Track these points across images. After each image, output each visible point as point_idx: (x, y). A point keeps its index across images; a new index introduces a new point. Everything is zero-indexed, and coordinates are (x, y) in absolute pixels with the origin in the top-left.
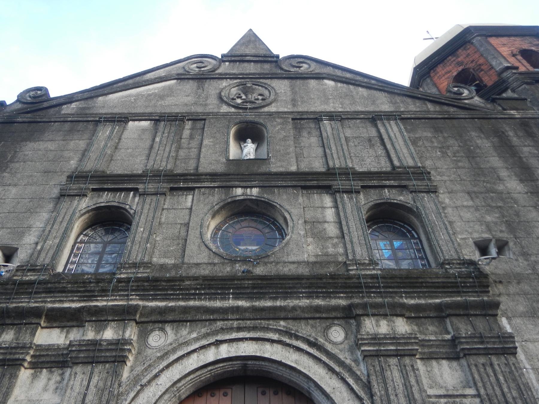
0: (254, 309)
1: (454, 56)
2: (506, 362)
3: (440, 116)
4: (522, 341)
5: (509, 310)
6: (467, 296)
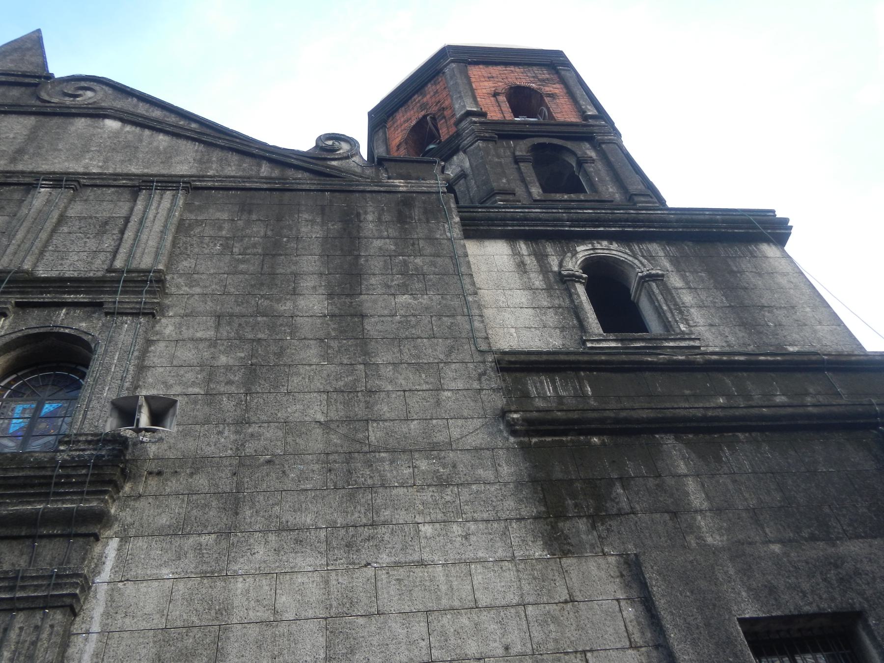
1: (421, 94)
2: (40, 624)
3: (265, 186)
4: (121, 581)
5: (137, 524)
6: (59, 501)
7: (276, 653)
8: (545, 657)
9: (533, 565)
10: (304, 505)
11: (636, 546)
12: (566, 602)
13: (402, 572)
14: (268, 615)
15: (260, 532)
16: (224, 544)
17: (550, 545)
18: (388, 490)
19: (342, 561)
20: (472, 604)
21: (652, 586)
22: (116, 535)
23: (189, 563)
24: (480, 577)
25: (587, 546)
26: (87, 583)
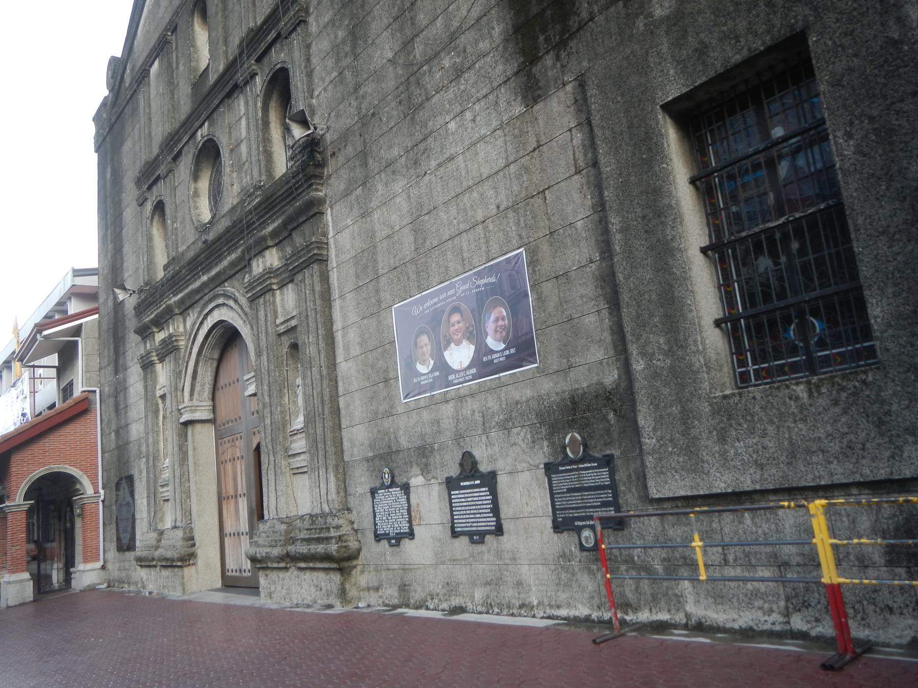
0: (212, 280)
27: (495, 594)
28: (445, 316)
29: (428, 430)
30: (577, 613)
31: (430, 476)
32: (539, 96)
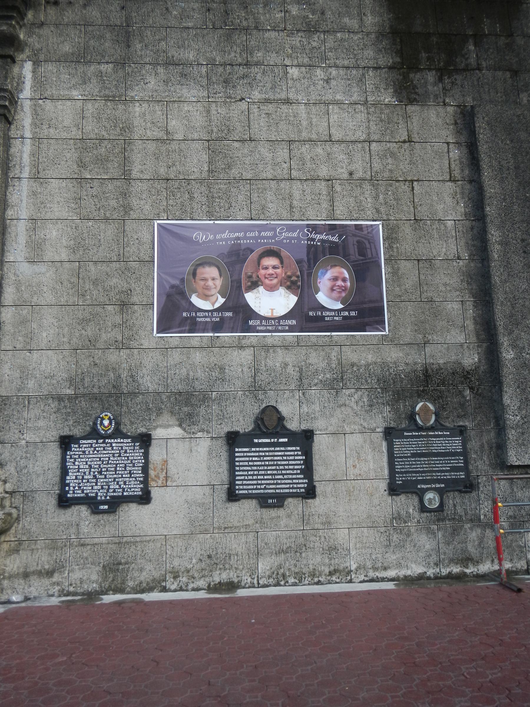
5: (44, 50)
7: (170, 164)
8: (380, 182)
9: (382, 109)
10: (186, 42)
11: (474, 99)
12: (404, 142)
13: (270, 108)
14: (162, 135)
15: (150, 64)
16: (121, 73)
17: (399, 93)
18: (261, 33)
19: (221, 95)
20: (327, 138)
21: (479, 133)
22: (29, 58)
23: (93, 87)
24: (336, 116)
25: (432, 96)
26: (14, 98)
27: (293, 562)
28: (253, 256)
29: (200, 374)
30: (409, 573)
31: (195, 428)
32: (415, 99)
